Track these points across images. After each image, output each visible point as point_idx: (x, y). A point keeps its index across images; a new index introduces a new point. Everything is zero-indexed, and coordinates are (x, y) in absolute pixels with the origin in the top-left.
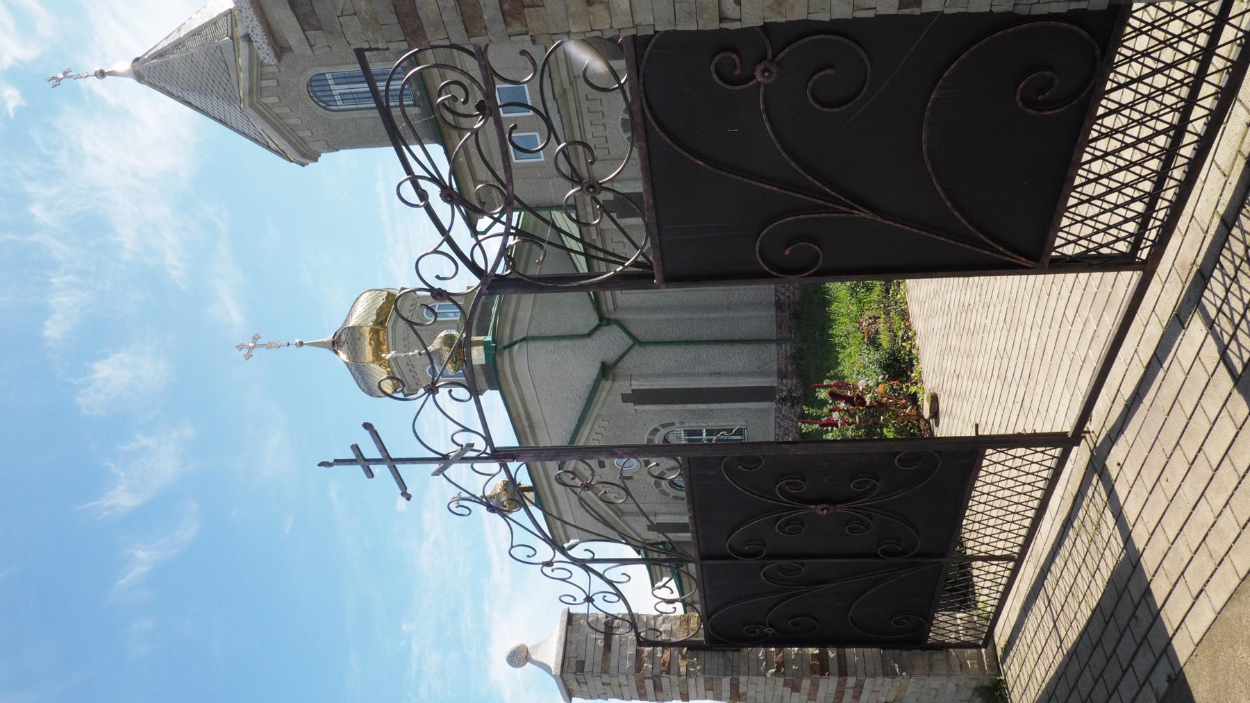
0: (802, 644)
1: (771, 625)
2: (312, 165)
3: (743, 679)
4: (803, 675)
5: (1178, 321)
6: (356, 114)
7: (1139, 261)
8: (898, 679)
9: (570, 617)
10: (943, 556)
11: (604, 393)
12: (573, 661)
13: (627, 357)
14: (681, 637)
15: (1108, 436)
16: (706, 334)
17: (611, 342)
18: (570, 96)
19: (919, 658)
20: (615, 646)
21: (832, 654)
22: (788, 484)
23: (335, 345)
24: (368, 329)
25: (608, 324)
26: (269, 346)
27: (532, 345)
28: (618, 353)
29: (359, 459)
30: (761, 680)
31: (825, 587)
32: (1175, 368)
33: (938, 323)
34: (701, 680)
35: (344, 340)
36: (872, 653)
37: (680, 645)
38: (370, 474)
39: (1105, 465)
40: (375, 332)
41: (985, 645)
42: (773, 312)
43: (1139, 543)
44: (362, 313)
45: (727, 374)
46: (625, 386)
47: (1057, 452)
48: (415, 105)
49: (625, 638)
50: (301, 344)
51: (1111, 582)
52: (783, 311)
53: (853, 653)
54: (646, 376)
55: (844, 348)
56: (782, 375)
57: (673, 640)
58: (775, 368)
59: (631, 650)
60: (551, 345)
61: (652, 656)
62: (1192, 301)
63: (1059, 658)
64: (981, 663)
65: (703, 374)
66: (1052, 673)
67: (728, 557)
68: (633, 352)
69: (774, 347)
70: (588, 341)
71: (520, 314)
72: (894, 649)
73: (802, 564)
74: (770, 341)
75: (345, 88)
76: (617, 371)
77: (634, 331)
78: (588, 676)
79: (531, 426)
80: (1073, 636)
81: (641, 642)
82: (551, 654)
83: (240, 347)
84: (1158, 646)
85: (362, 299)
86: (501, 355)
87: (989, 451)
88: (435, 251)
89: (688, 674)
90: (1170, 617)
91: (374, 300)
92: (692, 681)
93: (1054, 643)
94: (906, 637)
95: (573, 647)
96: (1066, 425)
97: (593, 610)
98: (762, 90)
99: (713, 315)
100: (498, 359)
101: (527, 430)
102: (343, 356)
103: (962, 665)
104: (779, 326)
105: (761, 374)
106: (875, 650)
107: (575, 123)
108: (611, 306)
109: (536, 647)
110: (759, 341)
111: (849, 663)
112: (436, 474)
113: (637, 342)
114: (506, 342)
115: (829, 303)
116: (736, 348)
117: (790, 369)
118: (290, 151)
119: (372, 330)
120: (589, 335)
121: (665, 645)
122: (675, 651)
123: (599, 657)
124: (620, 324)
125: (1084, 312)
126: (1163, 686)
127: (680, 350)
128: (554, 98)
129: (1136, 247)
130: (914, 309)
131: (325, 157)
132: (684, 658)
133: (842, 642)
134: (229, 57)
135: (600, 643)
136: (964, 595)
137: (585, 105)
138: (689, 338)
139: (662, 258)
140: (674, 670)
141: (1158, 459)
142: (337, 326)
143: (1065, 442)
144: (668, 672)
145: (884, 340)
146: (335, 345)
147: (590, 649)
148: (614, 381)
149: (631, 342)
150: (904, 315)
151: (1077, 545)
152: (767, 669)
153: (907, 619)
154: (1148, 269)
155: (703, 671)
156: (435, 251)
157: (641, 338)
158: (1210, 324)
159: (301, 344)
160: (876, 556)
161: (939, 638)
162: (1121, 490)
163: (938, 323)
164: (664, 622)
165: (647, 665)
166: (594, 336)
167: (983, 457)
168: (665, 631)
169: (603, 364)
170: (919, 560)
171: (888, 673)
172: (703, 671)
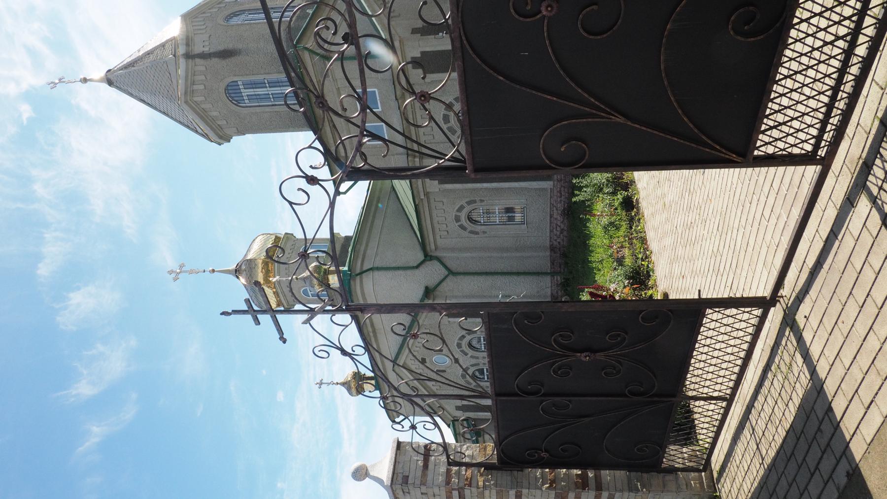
0: (569, 466)
1: (546, 451)
2: (226, 144)
3: (525, 491)
4: (569, 490)
5: (850, 202)
6: (258, 110)
7: (820, 158)
8: (640, 494)
9: (399, 445)
10: (674, 396)
12: (400, 476)
13: (444, 284)
14: (479, 460)
15: (797, 297)
16: (500, 266)
17: (432, 273)
19: (656, 479)
20: (431, 466)
21: (591, 474)
22: (561, 335)
23: (237, 272)
24: (260, 261)
25: (431, 260)
26: (191, 272)
27: (376, 273)
28: (437, 281)
29: (250, 311)
30: (538, 492)
31: (587, 420)
32: (848, 237)
33: (668, 241)
34: (494, 492)
35: (243, 269)
36: (621, 474)
37: (479, 465)
38: (257, 322)
39: (795, 320)
40: (266, 264)
41: (704, 470)
42: (548, 253)
43: (822, 374)
44: (256, 251)
47: (758, 312)
49: (439, 461)
50: (213, 271)
51: (801, 407)
53: (607, 475)
55: (599, 270)
57: (474, 462)
58: (549, 293)
59: (443, 469)
60: (390, 274)
61: (458, 473)
62: (859, 185)
63: (762, 472)
64: (701, 483)
66: (756, 484)
67: (517, 395)
68: (448, 280)
69: (548, 279)
70: (417, 272)
71: (368, 252)
72: (637, 471)
73: (570, 401)
74: (546, 274)
75: (251, 92)
76: (437, 293)
77: (448, 264)
78: (411, 487)
79: (374, 331)
80: (772, 453)
81: (451, 463)
82: (384, 471)
83: (171, 272)
84: (838, 449)
85: (257, 240)
86: (355, 280)
87: (709, 311)
88: (310, 147)
89: (485, 487)
90: (848, 426)
91: (266, 241)
92: (487, 493)
93: (757, 461)
94: (646, 462)
95: (401, 466)
96: (764, 291)
97: (417, 439)
98: (546, 21)
99: (505, 255)
100: (352, 282)
101: (371, 334)
102: (243, 280)
103: (688, 485)
104: (552, 263)
106: (623, 472)
108: (433, 247)
109: (373, 466)
111: (603, 481)
112: (305, 323)
113: (451, 272)
114: (358, 271)
115: (589, 239)
116: (521, 278)
117: (560, 294)
118: (211, 134)
119: (263, 262)
120: (417, 267)
121: (468, 465)
122: (475, 470)
123: (419, 473)
124: (439, 259)
125: (777, 210)
126: (842, 480)
127: (481, 279)
129: (817, 147)
130: (651, 236)
131: (236, 139)
132: (481, 475)
133: (597, 466)
134: (172, 68)
135: (421, 463)
136: (688, 434)
138: (488, 271)
139: (473, 158)
140: (474, 483)
141: (836, 307)
142: (239, 259)
143: (765, 304)
144: (470, 485)
145: (628, 261)
146: (237, 272)
147: (413, 467)
149: (447, 273)
150: (644, 241)
151: (774, 384)
152: (543, 484)
153: (647, 447)
154: (826, 164)
155: (496, 485)
156: (310, 147)
157: (454, 269)
158: (874, 200)
159: (213, 271)
160: (625, 396)
161: (670, 463)
162: (807, 336)
163: (668, 241)
164: (467, 449)
165: (455, 480)
166: (421, 268)
167: (704, 315)
168: (469, 456)
169: (427, 288)
170: (656, 399)
171: (632, 489)
172: (496, 485)
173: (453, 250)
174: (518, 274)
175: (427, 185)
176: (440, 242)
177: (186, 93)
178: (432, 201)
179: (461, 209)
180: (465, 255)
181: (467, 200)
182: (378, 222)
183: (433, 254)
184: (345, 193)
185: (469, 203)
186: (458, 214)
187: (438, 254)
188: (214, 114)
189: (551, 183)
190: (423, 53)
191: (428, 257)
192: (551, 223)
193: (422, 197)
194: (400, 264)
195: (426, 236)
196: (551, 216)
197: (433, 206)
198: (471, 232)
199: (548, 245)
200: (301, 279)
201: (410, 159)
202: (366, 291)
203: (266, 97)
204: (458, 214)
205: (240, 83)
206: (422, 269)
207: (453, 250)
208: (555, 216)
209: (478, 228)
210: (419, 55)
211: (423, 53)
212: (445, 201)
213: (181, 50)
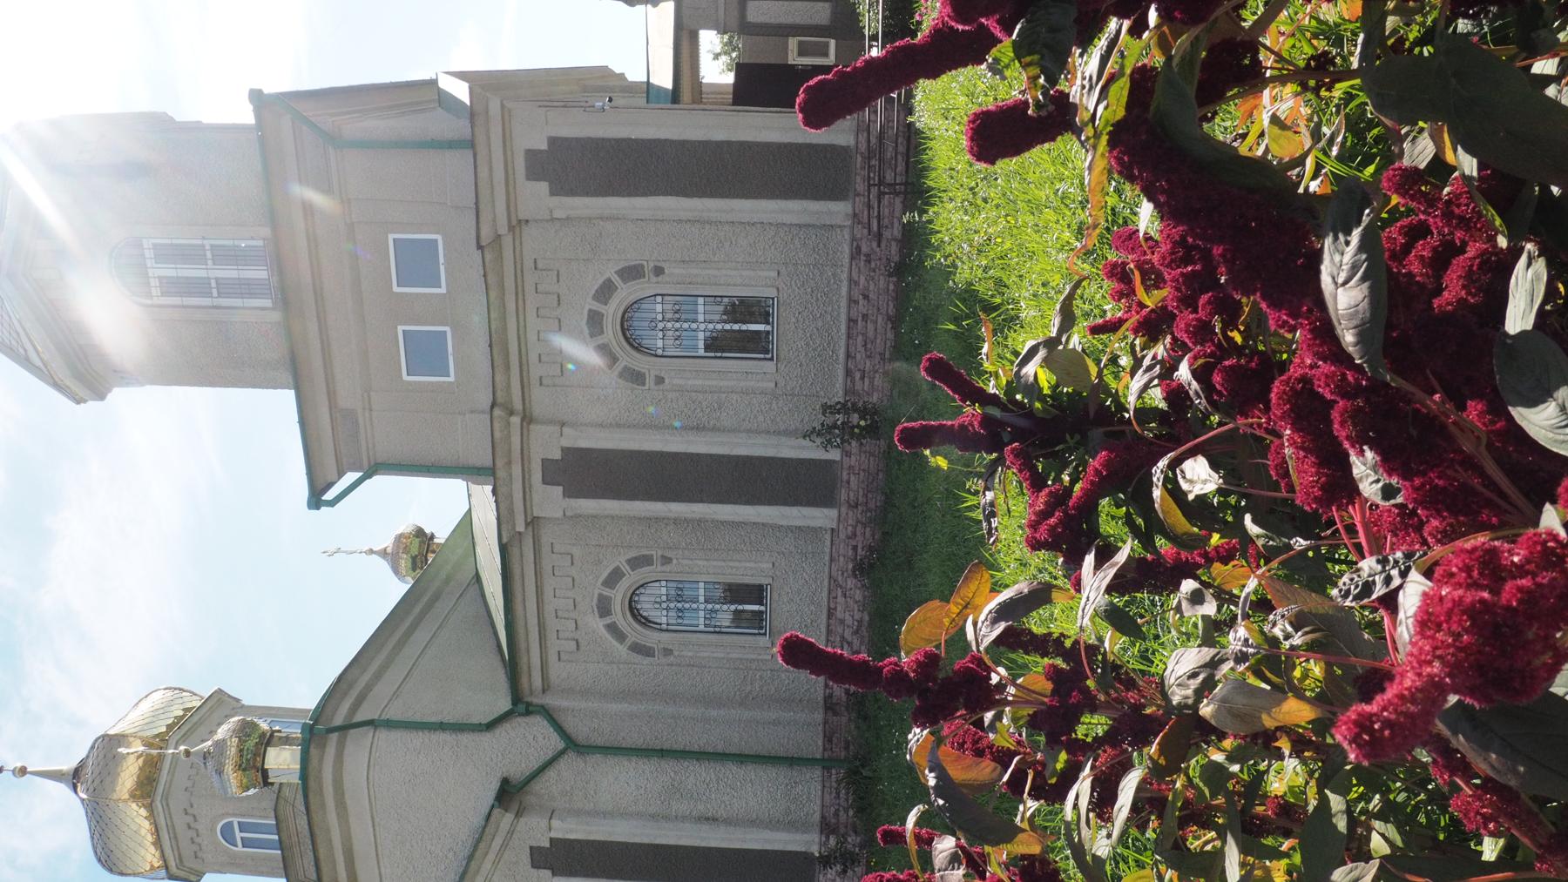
11: (498, 841)
13: (551, 774)
17: (528, 742)
18: (507, 241)
25: (528, 713)
27: (383, 735)
28: (536, 765)
42: (819, 716)
45: (729, 822)
46: (537, 830)
48: (273, 309)
52: (835, 714)
54: (578, 813)
56: (827, 828)
58: (817, 816)
60: (417, 739)
65: (684, 818)
68: (562, 764)
70: (486, 738)
76: (531, 799)
77: (571, 724)
86: (323, 746)
91: (170, 703)
99: (714, 713)
104: (828, 738)
105: (792, 825)
107: (511, 306)
110: (791, 761)
113: (573, 745)
114: (338, 721)
116: (751, 772)
117: (843, 817)
127: (647, 766)
128: (480, 247)
137: (530, 279)
148: (518, 815)
149: (561, 745)
157: (580, 729)
159: (23, 771)
169: (505, 782)
173: (585, 693)
174: (742, 758)
175: (536, 498)
176: (557, 671)
178: (546, 549)
179: (614, 578)
180: (614, 707)
181: (633, 554)
182: (421, 636)
183: (535, 701)
184: (332, 503)
185: (636, 563)
186: (607, 592)
187: (549, 700)
189: (833, 513)
190: (553, 141)
191: (521, 706)
192: (829, 632)
193: (520, 527)
194: (448, 718)
195: (523, 646)
196: (830, 615)
197: (547, 565)
198: (637, 648)
199: (820, 698)
200: (196, 753)
201: (497, 412)
202: (347, 784)
204: (607, 592)
206: (502, 732)
207: (585, 693)
208: (839, 614)
209: (652, 638)
210: (544, 146)
211: (553, 141)
212: (576, 552)
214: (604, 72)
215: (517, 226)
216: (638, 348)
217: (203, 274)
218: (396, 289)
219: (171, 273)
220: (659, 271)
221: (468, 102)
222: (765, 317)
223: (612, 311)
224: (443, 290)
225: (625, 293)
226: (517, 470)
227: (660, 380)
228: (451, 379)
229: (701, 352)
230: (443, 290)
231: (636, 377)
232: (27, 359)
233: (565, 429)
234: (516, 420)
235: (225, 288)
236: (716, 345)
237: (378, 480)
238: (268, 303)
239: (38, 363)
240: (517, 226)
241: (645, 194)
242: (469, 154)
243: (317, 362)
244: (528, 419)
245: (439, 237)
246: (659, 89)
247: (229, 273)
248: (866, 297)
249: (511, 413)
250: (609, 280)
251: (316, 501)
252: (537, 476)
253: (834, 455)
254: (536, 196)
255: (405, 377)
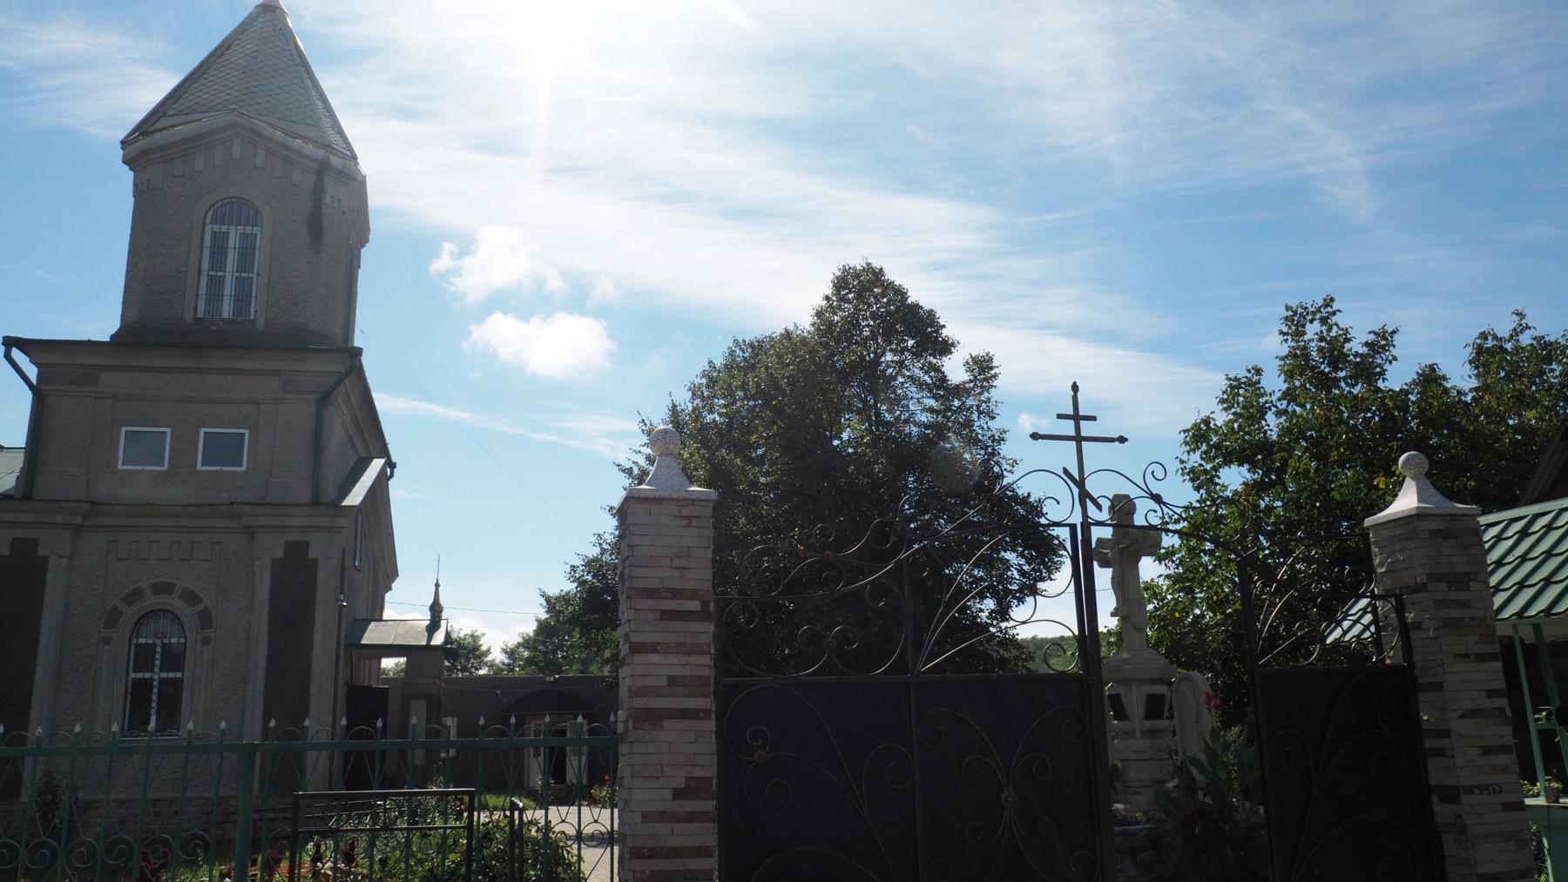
48: (195, 318)
128: (232, 504)
131: (128, 175)
177: (254, 132)
184: (8, 357)
188: (200, 162)
190: (315, 562)
201: (86, 506)
203: (218, 261)
205: (257, 230)
210: (311, 556)
211: (315, 562)
213: (335, 161)
214: (392, 573)
215: (250, 532)
216: (139, 622)
217: (229, 268)
218: (203, 430)
219: (231, 244)
220: (206, 641)
221: (346, 503)
222: (160, 729)
223: (174, 602)
224: (199, 467)
225: (189, 614)
226: (28, 517)
227: (107, 641)
228: (120, 466)
229: (133, 676)
230: (199, 467)
231: (112, 620)
232: (164, 115)
233: (64, 562)
234: (78, 520)
235: (216, 284)
236: (140, 691)
237: (28, 396)
238: (200, 314)
239: (158, 125)
240: (250, 532)
241: (269, 631)
242: (306, 498)
243: (143, 362)
244: (78, 530)
245: (244, 468)
246: (364, 631)
247: (229, 288)
248: (176, 813)
249: (85, 517)
250: (201, 601)
251: (10, 342)
252: (20, 534)
253: (25, 797)
254: (274, 547)
255: (124, 429)
